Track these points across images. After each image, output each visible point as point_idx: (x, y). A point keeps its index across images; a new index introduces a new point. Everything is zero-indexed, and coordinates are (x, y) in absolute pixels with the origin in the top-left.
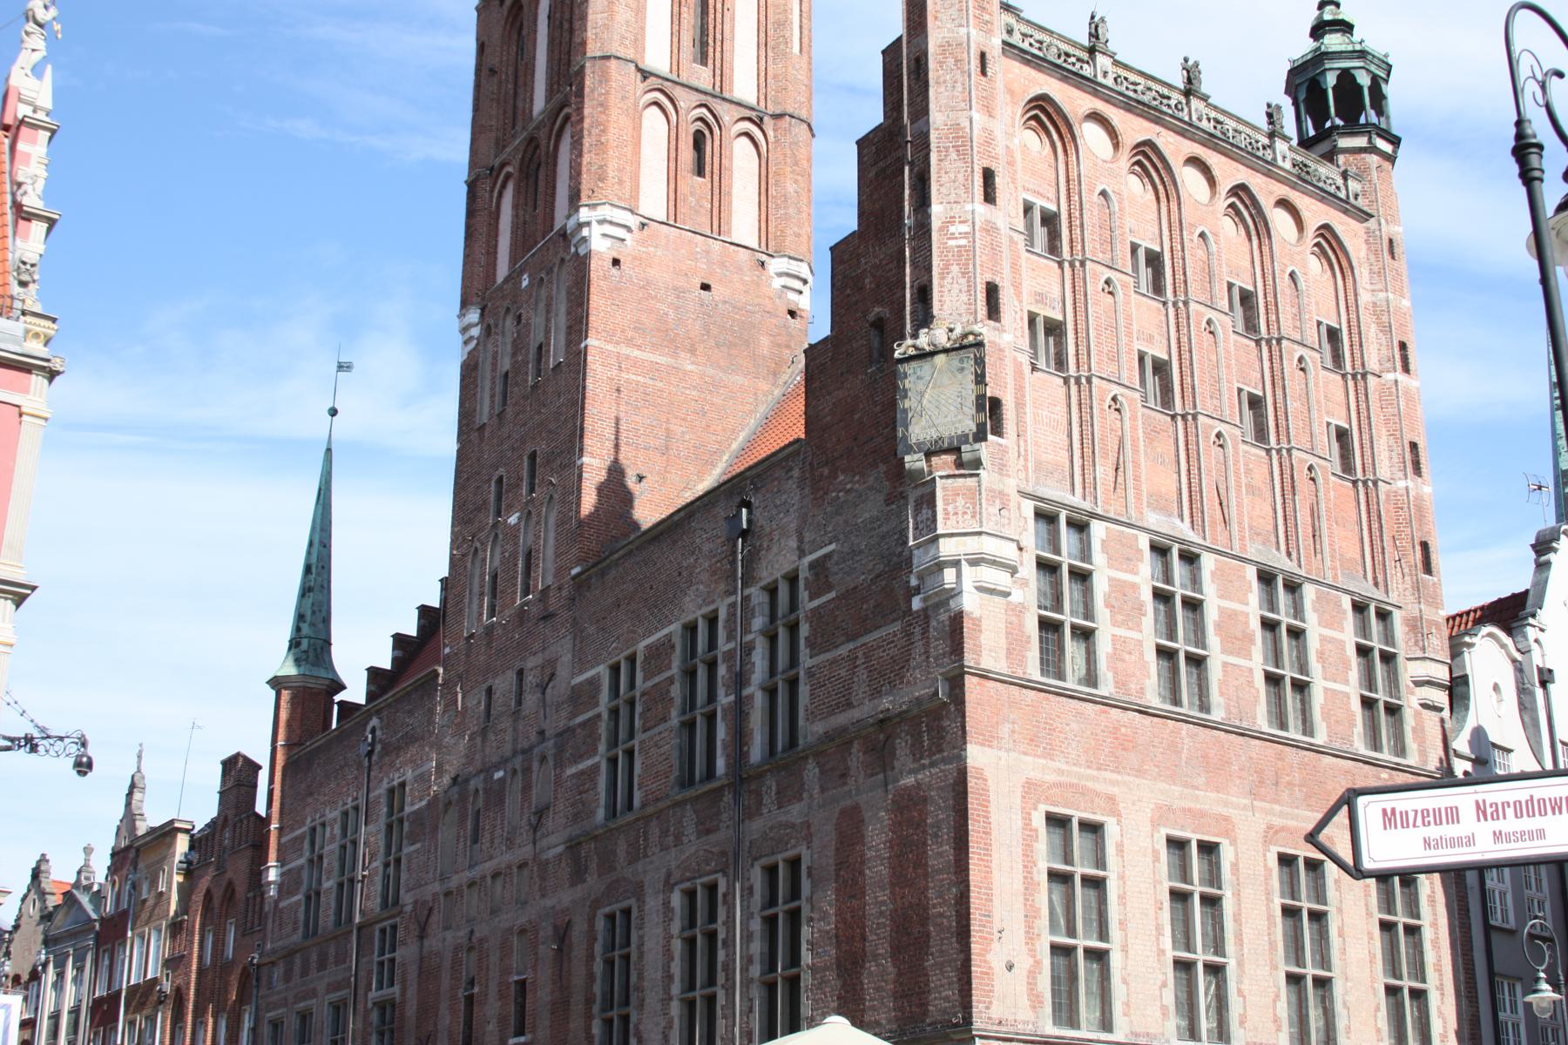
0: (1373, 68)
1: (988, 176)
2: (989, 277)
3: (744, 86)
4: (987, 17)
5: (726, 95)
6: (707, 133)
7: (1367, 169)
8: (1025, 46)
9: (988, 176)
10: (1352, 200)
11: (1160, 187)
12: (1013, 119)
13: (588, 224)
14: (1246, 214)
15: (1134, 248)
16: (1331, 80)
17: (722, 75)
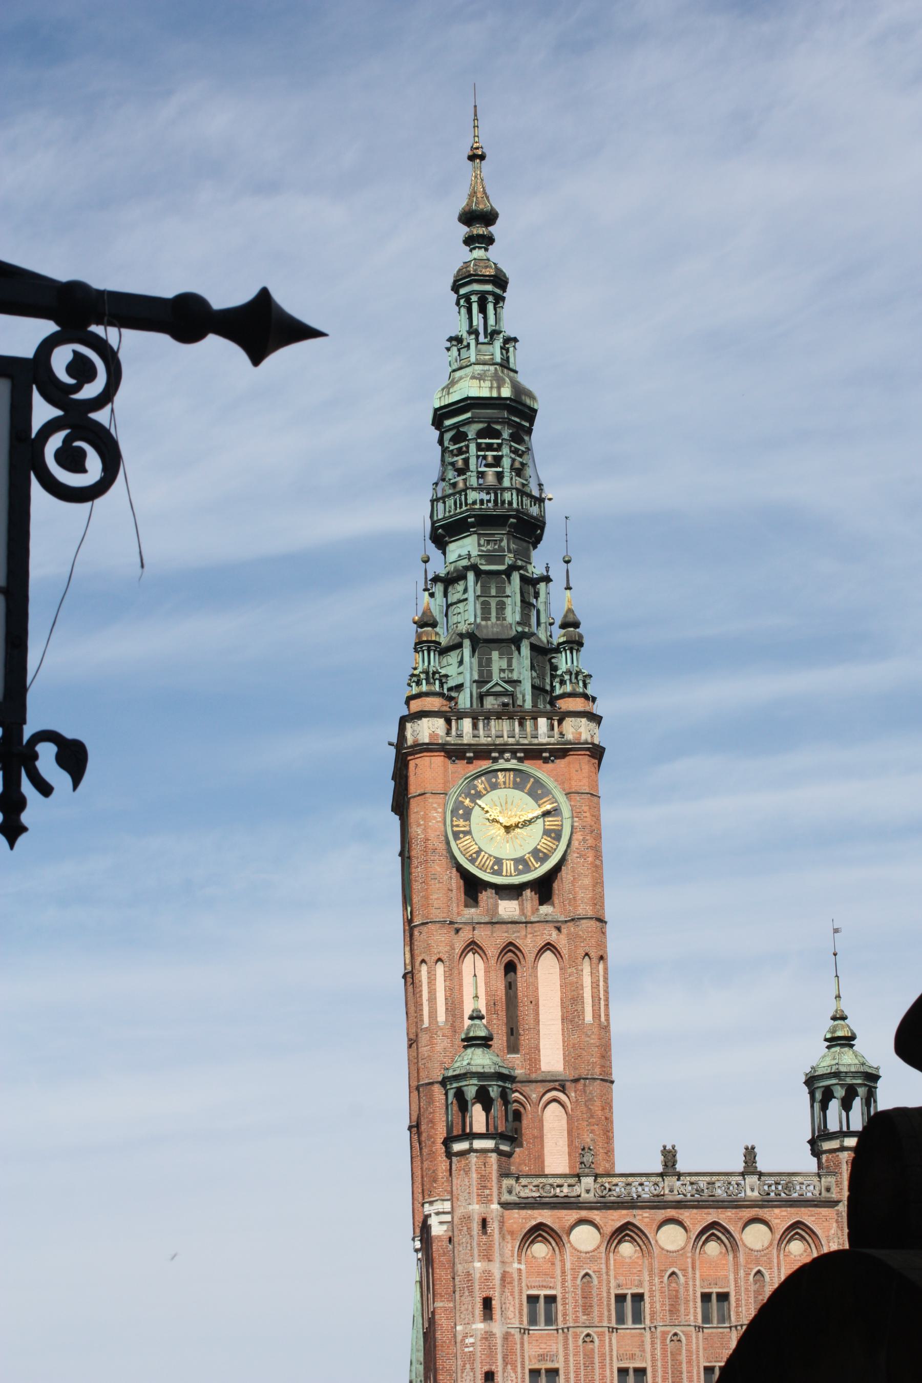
0: (849, 1081)
1: (487, 1303)
2: (486, 1368)
3: (552, 1058)
4: (487, 1192)
5: (533, 1076)
6: (522, 1110)
7: (838, 1165)
8: (525, 1193)
9: (487, 1303)
10: (824, 1193)
11: (643, 1247)
12: (512, 1251)
13: (430, 1215)
14: (723, 1238)
15: (621, 1298)
16: (818, 1095)
17: (534, 1059)
